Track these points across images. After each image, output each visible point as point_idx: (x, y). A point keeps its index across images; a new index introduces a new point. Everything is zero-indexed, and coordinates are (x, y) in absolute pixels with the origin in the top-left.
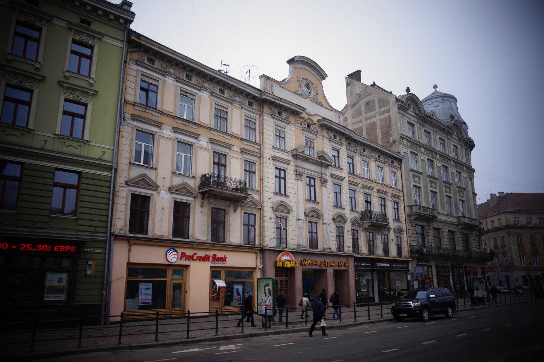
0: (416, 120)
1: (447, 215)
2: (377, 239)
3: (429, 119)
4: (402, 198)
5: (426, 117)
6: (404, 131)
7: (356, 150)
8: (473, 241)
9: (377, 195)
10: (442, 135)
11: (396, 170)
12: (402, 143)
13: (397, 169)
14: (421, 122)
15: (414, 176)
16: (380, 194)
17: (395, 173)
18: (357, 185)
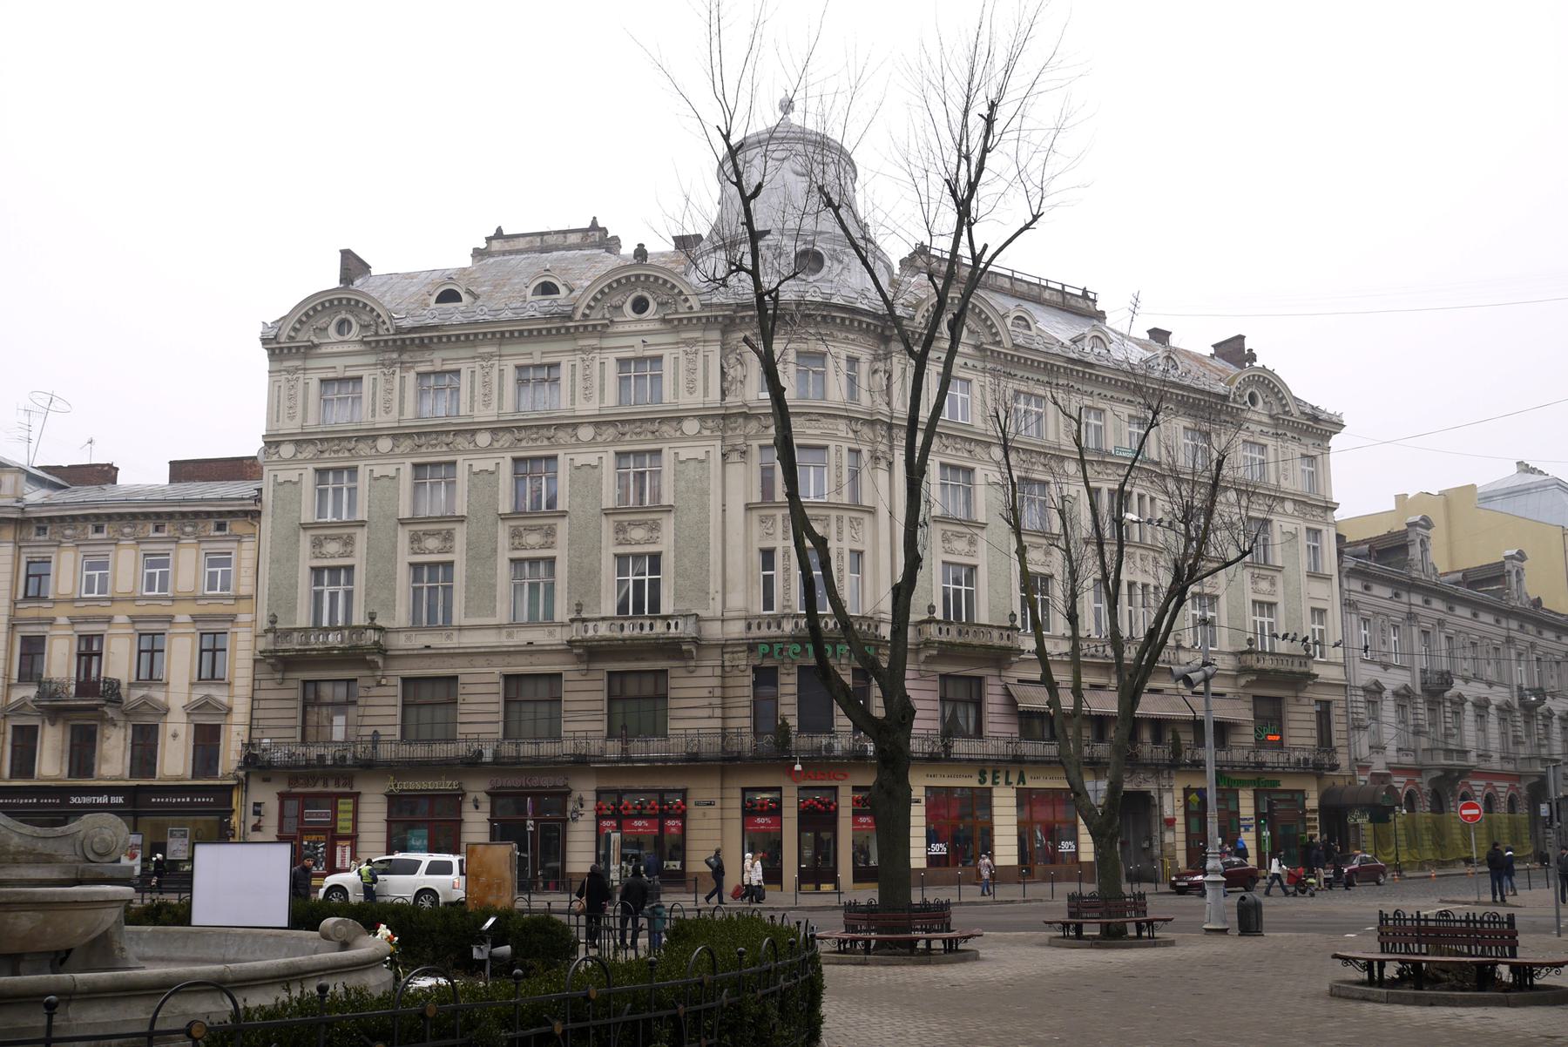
0: (371, 359)
1: (498, 627)
2: (108, 738)
3: (423, 335)
4: (244, 618)
5: (405, 333)
6: (292, 417)
7: (64, 536)
8: (705, 693)
9: (131, 631)
10: (531, 354)
11: (235, 545)
12: (275, 458)
13: (239, 541)
14: (395, 356)
15: (317, 543)
16: (139, 626)
17: (230, 553)
18: (51, 621)
